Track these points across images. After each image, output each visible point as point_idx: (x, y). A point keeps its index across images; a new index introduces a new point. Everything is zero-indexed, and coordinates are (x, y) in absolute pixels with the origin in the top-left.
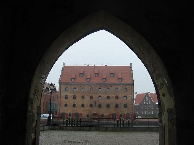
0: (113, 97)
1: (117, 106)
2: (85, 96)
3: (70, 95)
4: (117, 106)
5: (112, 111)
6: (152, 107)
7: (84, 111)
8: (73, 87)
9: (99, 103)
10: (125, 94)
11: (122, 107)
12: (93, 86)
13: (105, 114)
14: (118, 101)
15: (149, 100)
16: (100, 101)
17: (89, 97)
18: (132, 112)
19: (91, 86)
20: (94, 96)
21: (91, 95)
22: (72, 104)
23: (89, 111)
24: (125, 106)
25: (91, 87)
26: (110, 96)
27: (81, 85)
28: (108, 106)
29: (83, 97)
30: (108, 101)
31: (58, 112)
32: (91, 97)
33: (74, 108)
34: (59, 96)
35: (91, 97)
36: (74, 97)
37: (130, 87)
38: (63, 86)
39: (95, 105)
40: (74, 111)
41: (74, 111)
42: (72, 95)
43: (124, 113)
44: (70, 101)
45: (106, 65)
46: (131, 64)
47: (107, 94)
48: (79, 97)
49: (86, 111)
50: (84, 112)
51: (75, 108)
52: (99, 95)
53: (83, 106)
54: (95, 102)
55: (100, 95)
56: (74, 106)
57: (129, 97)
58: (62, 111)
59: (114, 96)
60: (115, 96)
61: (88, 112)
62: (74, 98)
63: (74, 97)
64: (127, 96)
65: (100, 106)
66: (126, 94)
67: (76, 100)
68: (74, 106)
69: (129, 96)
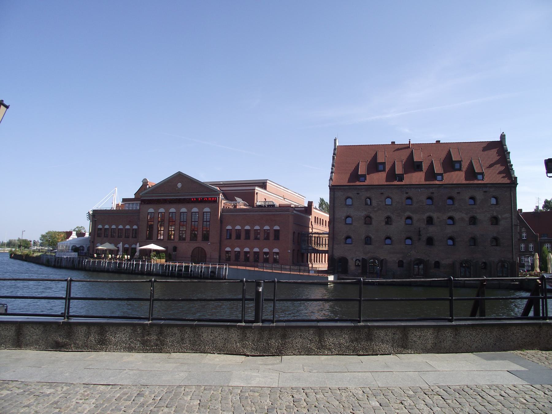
1: (474, 241)
2: (393, 217)
6: (531, 246)
9: (428, 235)
13: (443, 262)
15: (523, 230)
17: (404, 218)
19: (407, 193)
20: (415, 217)
21: (408, 214)
22: (363, 237)
24: (496, 241)
25: (407, 195)
29: (388, 220)
30: (450, 230)
33: (366, 246)
36: (368, 220)
38: (339, 194)
39: (420, 239)
42: (364, 213)
45: (438, 142)
46: (503, 137)
48: (378, 218)
51: (370, 246)
52: (427, 214)
54: (420, 231)
55: (431, 214)
56: (368, 241)
59: (466, 218)
63: (368, 220)
64: (499, 216)
65: (430, 241)
68: (368, 241)
69: (503, 216)
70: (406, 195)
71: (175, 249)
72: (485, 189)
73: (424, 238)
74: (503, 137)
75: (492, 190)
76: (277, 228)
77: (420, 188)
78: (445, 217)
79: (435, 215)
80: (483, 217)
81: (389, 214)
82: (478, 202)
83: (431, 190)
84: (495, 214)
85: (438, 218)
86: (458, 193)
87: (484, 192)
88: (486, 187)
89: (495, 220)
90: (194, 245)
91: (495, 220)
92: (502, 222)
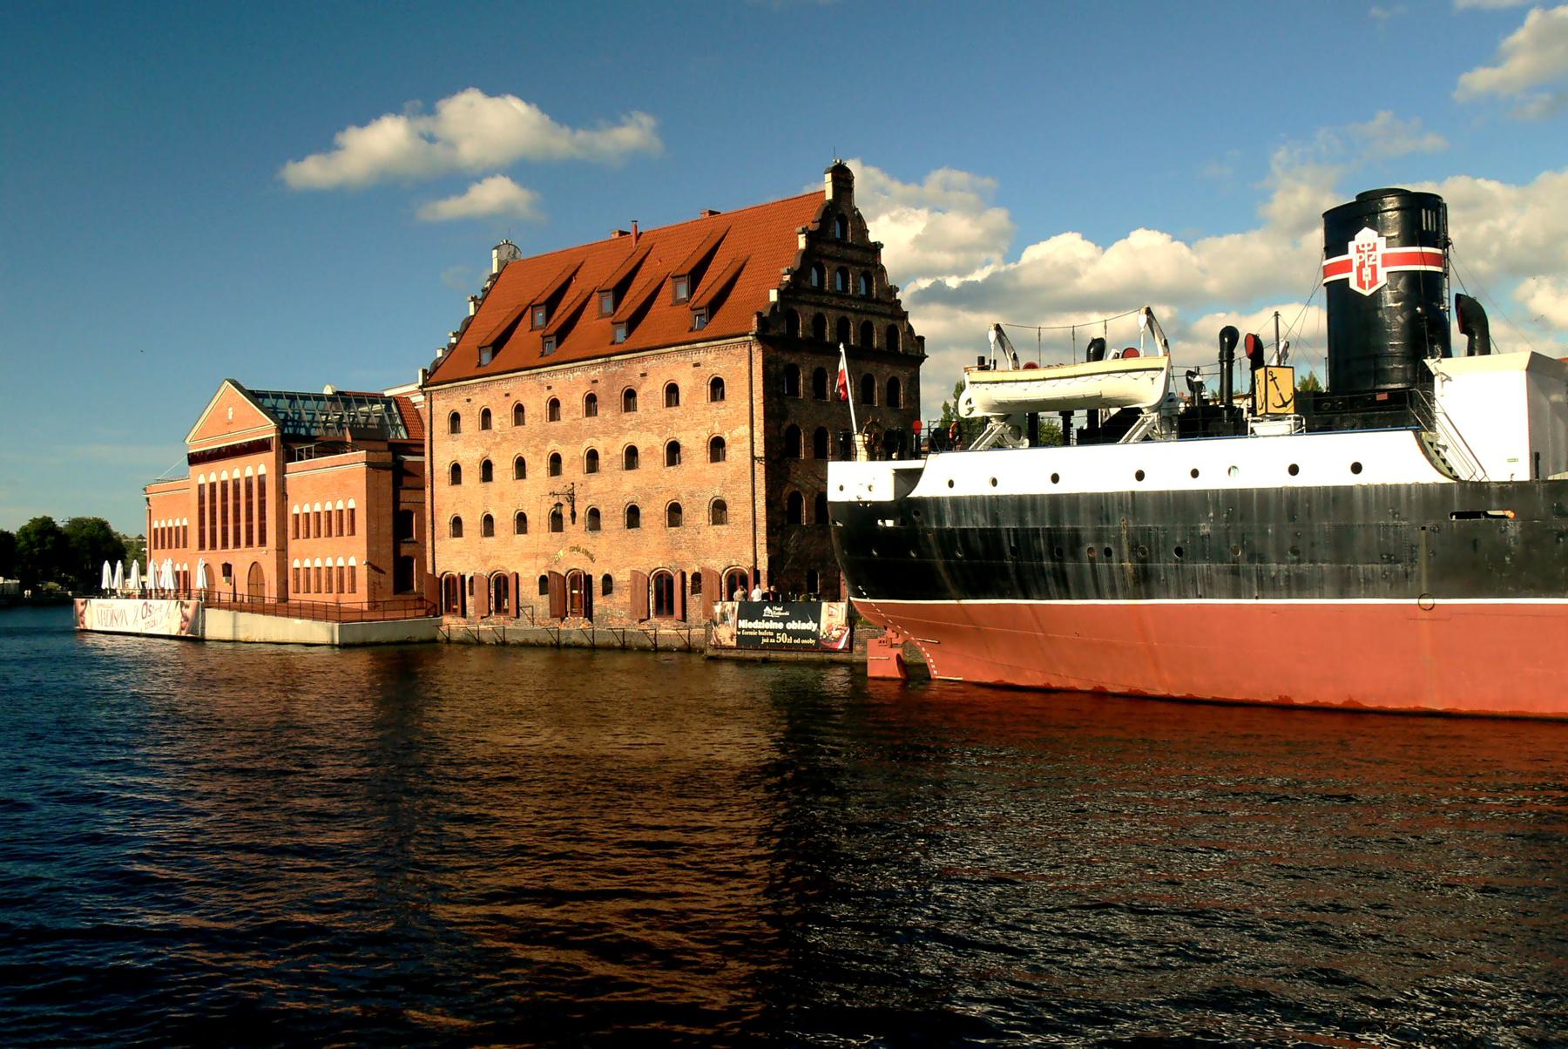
0: (651, 451)
4: (675, 513)
5: (649, 552)
7: (528, 556)
10: (713, 419)
16: (596, 482)
21: (553, 446)
23: (547, 555)
27: (506, 387)
29: (521, 466)
31: (429, 570)
34: (427, 469)
35: (556, 461)
37: (744, 365)
40: (489, 558)
41: (489, 558)
47: (621, 430)
49: (537, 556)
50: (529, 563)
53: (521, 522)
57: (737, 440)
61: (542, 562)
64: (727, 437)
66: (723, 422)
67: (489, 484)
69: (735, 433)
70: (547, 395)
72: (696, 358)
73: (581, 513)
75: (710, 357)
76: (352, 504)
78: (619, 450)
80: (694, 444)
82: (683, 396)
83: (594, 373)
84: (717, 432)
85: (607, 453)
86: (643, 375)
89: (717, 447)
91: (717, 447)
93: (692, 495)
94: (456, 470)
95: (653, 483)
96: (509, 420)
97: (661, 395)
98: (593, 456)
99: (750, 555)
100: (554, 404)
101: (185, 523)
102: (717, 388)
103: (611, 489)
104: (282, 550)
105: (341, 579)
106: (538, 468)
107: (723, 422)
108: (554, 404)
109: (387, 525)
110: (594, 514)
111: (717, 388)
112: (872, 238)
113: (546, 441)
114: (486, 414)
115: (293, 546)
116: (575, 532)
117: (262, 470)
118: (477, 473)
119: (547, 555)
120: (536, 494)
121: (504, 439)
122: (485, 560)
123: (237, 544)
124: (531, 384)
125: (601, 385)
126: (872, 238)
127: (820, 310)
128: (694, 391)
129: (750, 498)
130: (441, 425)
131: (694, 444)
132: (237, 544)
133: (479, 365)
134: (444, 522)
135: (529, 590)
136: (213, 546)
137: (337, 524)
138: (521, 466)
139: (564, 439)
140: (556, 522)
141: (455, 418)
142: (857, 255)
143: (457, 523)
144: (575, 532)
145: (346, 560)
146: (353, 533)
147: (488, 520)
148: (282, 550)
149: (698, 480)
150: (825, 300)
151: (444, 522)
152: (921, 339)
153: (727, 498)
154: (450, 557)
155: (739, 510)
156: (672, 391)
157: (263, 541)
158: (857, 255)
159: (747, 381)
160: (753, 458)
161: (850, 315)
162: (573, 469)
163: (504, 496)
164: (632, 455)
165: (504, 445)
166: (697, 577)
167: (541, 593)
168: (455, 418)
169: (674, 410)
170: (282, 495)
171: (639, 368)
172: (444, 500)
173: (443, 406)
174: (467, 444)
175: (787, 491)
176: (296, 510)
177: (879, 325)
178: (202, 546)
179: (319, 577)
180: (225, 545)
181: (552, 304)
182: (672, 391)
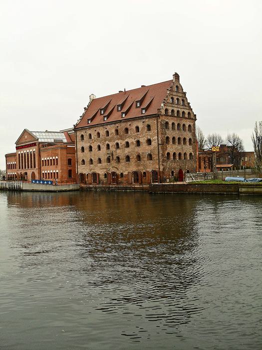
1: (139, 157)
3: (86, 145)
4: (139, 157)
5: (133, 168)
8: (89, 132)
11: (145, 159)
12: (108, 127)
13: (124, 173)
14: (140, 150)
16: (118, 151)
18: (159, 169)
21: (107, 142)
23: (106, 169)
24: (150, 157)
26: (130, 141)
27: (95, 129)
28: (128, 158)
29: (99, 147)
32: (108, 145)
33: (91, 165)
36: (91, 147)
37: (155, 122)
42: (88, 145)
43: (148, 170)
44: (87, 156)
48: (95, 147)
49: (104, 169)
50: (101, 170)
52: (116, 142)
53: (100, 161)
57: (154, 140)
58: (80, 171)
59: (134, 141)
60: (136, 140)
62: (89, 151)
63: (91, 147)
66: (150, 136)
71: (26, 173)
72: (143, 120)
73: (115, 158)
74: (177, 76)
75: (147, 120)
76: (57, 157)
77: (112, 124)
78: (124, 143)
79: (119, 142)
80: (143, 140)
81: (99, 144)
83: (117, 125)
87: (143, 122)
88: (144, 119)
89: (149, 142)
90: (32, 171)
91: (149, 142)
92: (153, 143)
93: (143, 153)
94: (83, 149)
95: (132, 150)
96: (96, 137)
97: (135, 130)
98: (117, 144)
99: (158, 167)
100: (107, 132)
101: (15, 163)
102: (149, 127)
103: (122, 153)
104: (40, 169)
105: (55, 175)
106: (104, 148)
107: (150, 136)
108: (107, 132)
109: (66, 162)
110: (118, 158)
111: (149, 127)
112: (184, 91)
113: (106, 141)
114: (90, 135)
115: (42, 168)
116: (113, 163)
117: (34, 150)
118: (88, 150)
119: (106, 169)
120: (103, 154)
121: (95, 141)
122: (91, 170)
123: (28, 168)
124: (101, 128)
125: (119, 128)
126: (184, 91)
127: (173, 108)
128: (143, 128)
129: (157, 153)
130: (79, 138)
131: (143, 140)
132: (28, 168)
133: (88, 124)
134: (80, 161)
135: (102, 177)
136: (22, 168)
137: (54, 162)
138: (99, 147)
139: (110, 141)
140: (109, 160)
141: (82, 136)
142: (181, 95)
143: (83, 161)
144: (113, 163)
145: (56, 171)
146: (57, 164)
147: (91, 160)
148: (40, 169)
149: (144, 149)
150: (174, 106)
151: (80, 161)
152: (195, 115)
153: (152, 154)
154: (82, 169)
155: (155, 157)
156: (137, 128)
157: (35, 167)
158: (181, 95)
159: (156, 126)
160: (158, 144)
161: (179, 109)
162: (112, 149)
163: (95, 154)
164: (127, 145)
165: (95, 142)
166: (144, 173)
167: (105, 177)
168: (82, 136)
169: (138, 133)
170: (40, 156)
171: (129, 123)
172: (80, 155)
173: (79, 134)
174: (86, 142)
175: (166, 152)
176: (43, 159)
177: (187, 112)
178: (20, 168)
179: (55, 174)
180: (25, 168)
181: (105, 109)
182: (137, 128)
